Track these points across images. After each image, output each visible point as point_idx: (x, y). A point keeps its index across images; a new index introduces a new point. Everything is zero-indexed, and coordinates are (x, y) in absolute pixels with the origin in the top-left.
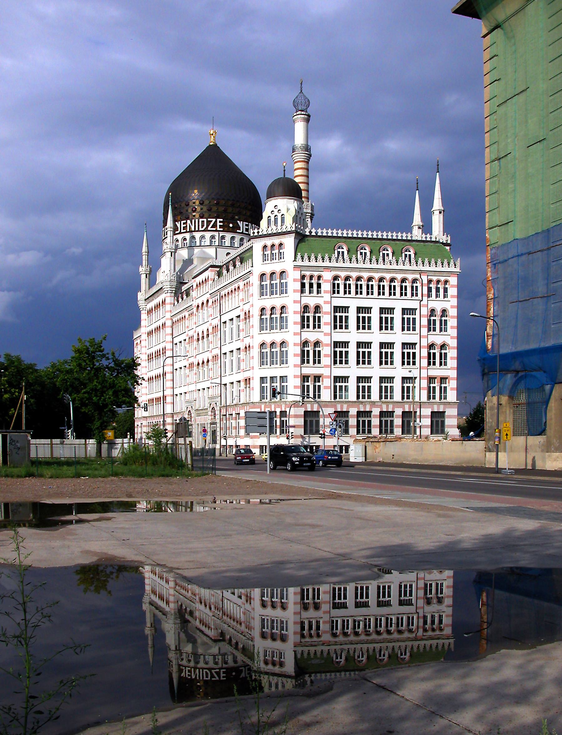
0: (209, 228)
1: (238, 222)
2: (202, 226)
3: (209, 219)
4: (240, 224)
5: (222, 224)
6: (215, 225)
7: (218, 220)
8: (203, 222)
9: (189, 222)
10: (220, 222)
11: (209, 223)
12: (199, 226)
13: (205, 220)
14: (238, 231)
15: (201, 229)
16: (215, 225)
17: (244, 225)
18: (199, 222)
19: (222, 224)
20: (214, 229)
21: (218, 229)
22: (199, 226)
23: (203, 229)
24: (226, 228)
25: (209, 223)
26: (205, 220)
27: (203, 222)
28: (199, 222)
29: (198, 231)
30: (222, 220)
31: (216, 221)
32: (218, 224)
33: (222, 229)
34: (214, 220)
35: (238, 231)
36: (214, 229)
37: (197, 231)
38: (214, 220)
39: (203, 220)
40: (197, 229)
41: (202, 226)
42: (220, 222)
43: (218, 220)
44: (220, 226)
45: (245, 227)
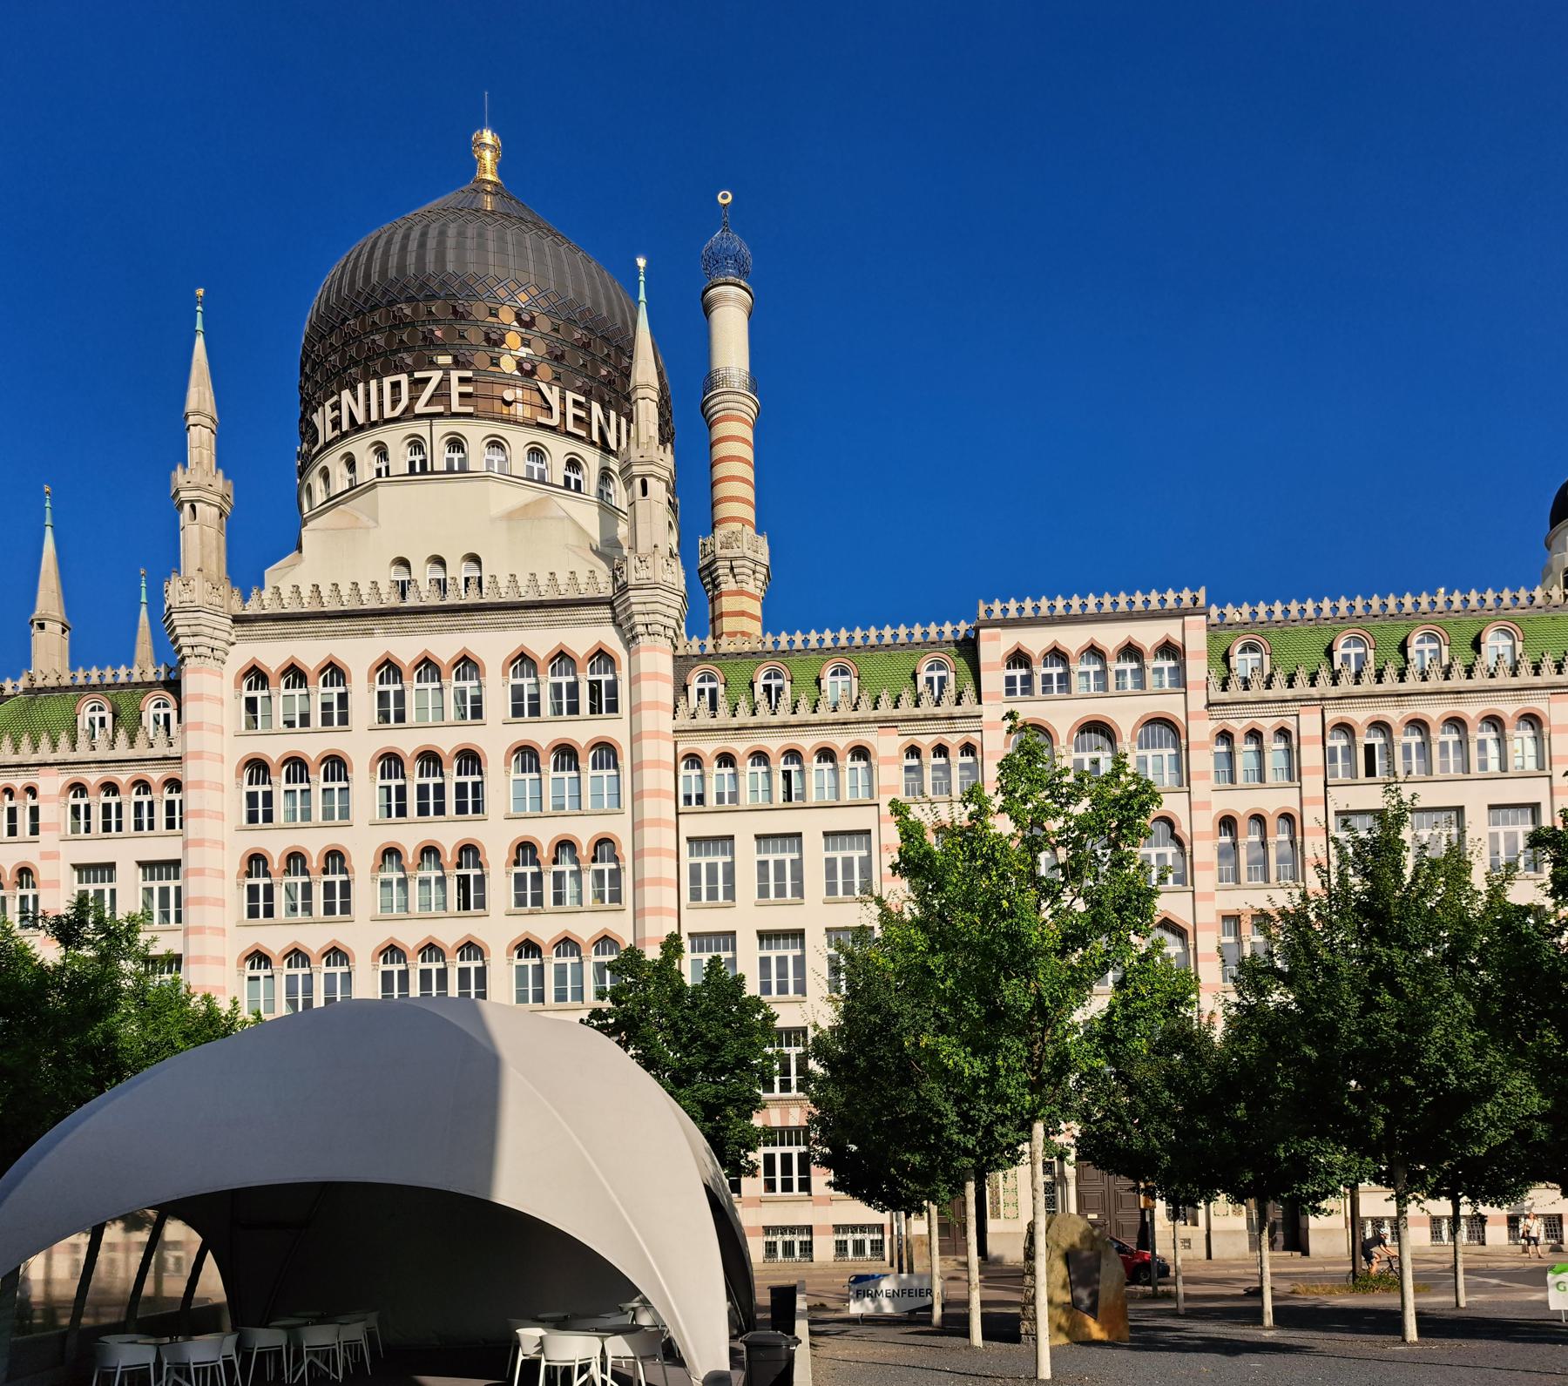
0: (420, 408)
1: (543, 387)
3: (417, 375)
4: (553, 396)
7: (455, 375)
8: (396, 386)
9: (346, 395)
12: (381, 405)
13: (404, 379)
14: (541, 420)
15: (388, 414)
16: (441, 394)
17: (569, 403)
18: (380, 390)
20: (440, 409)
21: (456, 408)
22: (381, 405)
23: (397, 413)
26: (404, 379)
27: (396, 386)
28: (380, 390)
32: (456, 389)
37: (374, 425)
39: (394, 378)
40: (374, 417)
43: (455, 375)
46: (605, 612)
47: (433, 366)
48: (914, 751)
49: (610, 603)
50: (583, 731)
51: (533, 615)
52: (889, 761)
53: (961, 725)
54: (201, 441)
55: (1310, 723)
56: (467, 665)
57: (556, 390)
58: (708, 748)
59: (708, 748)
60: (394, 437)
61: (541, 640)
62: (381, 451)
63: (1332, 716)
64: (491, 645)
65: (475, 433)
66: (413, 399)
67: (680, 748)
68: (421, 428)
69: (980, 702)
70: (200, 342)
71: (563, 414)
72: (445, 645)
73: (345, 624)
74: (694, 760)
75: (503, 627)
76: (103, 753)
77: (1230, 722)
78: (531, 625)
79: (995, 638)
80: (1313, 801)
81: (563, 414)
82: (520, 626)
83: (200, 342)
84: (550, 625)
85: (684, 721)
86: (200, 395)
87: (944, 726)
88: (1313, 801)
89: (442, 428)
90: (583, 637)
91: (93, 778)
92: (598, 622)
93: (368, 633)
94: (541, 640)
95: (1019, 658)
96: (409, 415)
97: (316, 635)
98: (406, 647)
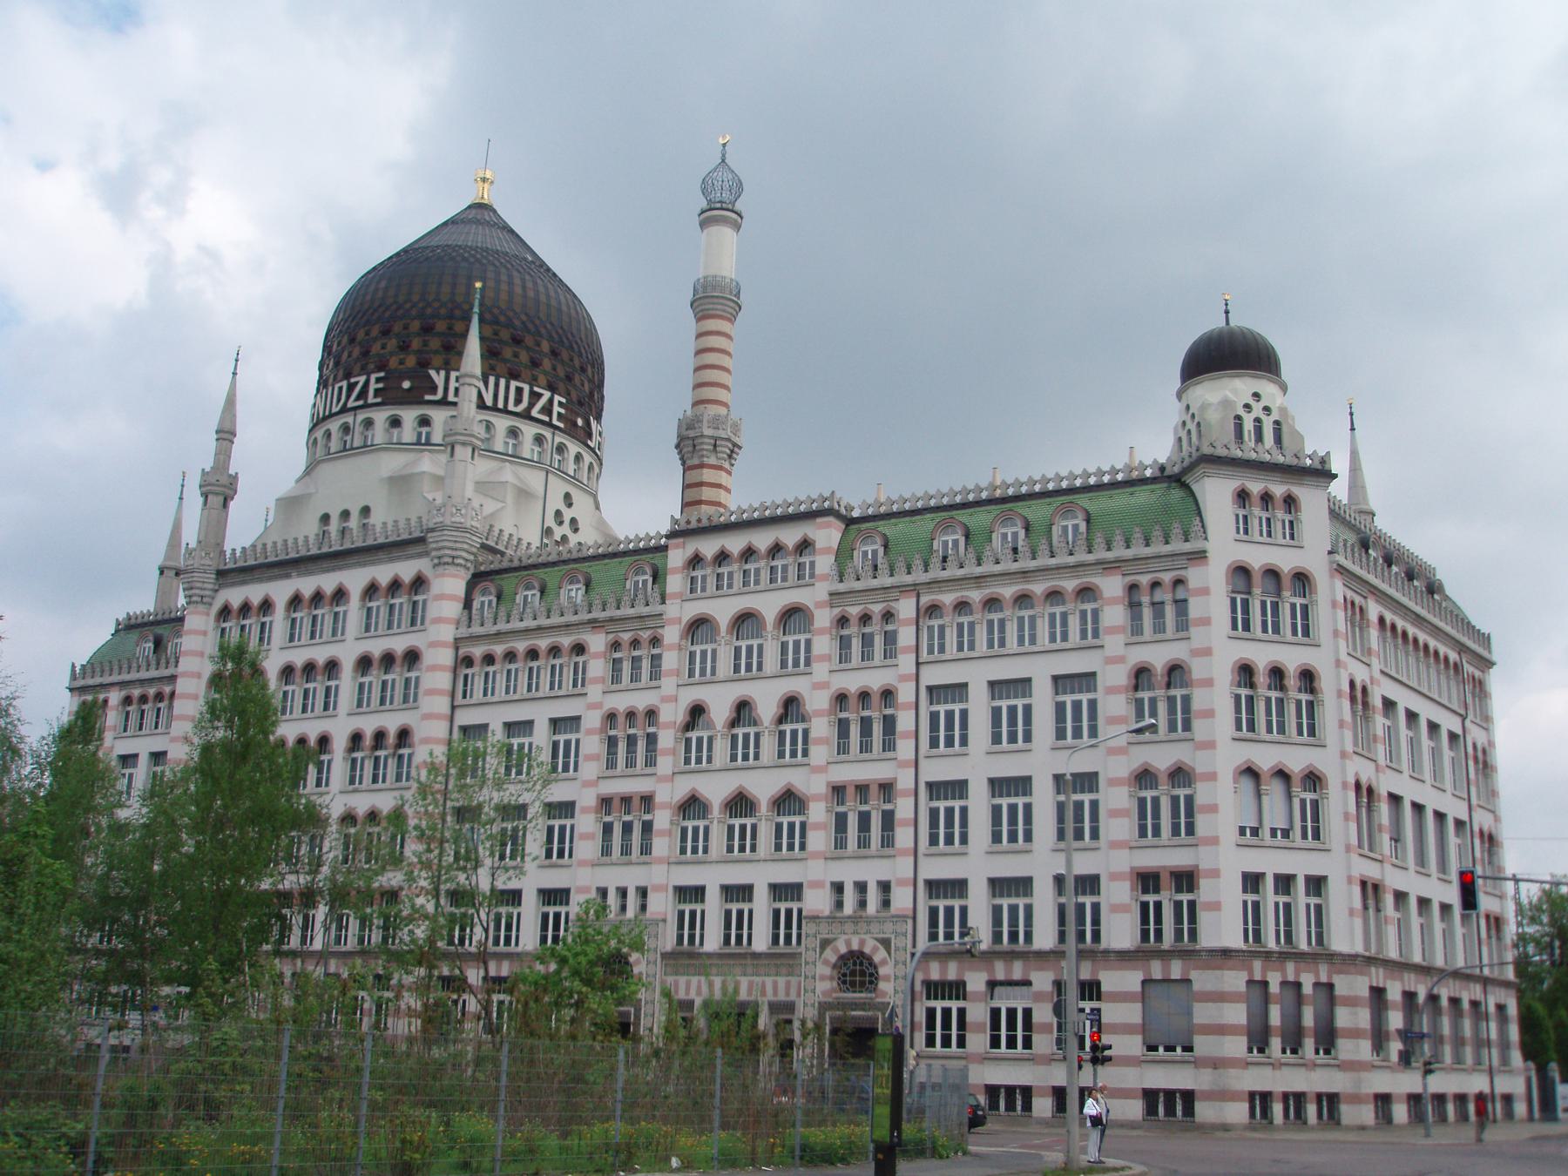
1: (432, 373)
2: (339, 400)
6: (363, 394)
10: (378, 380)
11: (351, 387)
13: (344, 384)
14: (428, 397)
19: (380, 385)
20: (361, 403)
21: (371, 400)
24: (390, 396)
25: (351, 387)
26: (344, 384)
29: (332, 415)
30: (382, 374)
31: (367, 384)
32: (373, 386)
33: (379, 400)
34: (362, 379)
35: (428, 397)
36: (361, 403)
38: (362, 379)
41: (339, 400)
42: (378, 380)
44: (377, 392)
45: (453, 385)
46: (419, 549)
47: (365, 370)
48: (616, 646)
49: (421, 540)
50: (399, 645)
51: (381, 555)
52: (596, 656)
53: (651, 623)
55: (906, 608)
56: (340, 595)
57: (443, 373)
58: (478, 651)
59: (478, 651)
60: (334, 426)
61: (383, 573)
62: (328, 435)
63: (926, 599)
64: (355, 579)
65: (381, 417)
66: (348, 397)
67: (461, 652)
68: (349, 418)
69: (663, 602)
71: (446, 389)
72: (328, 582)
73: (276, 571)
74: (468, 661)
75: (364, 565)
76: (144, 675)
77: (871, 607)
78: (380, 562)
79: (677, 547)
80: (903, 678)
81: (446, 389)
82: (373, 563)
84: (391, 560)
85: (464, 632)
87: (636, 625)
88: (903, 678)
89: (361, 416)
90: (405, 570)
91: (136, 692)
92: (420, 555)
93: (288, 576)
94: (383, 573)
95: (696, 561)
96: (344, 410)
97: (260, 580)
98: (306, 585)
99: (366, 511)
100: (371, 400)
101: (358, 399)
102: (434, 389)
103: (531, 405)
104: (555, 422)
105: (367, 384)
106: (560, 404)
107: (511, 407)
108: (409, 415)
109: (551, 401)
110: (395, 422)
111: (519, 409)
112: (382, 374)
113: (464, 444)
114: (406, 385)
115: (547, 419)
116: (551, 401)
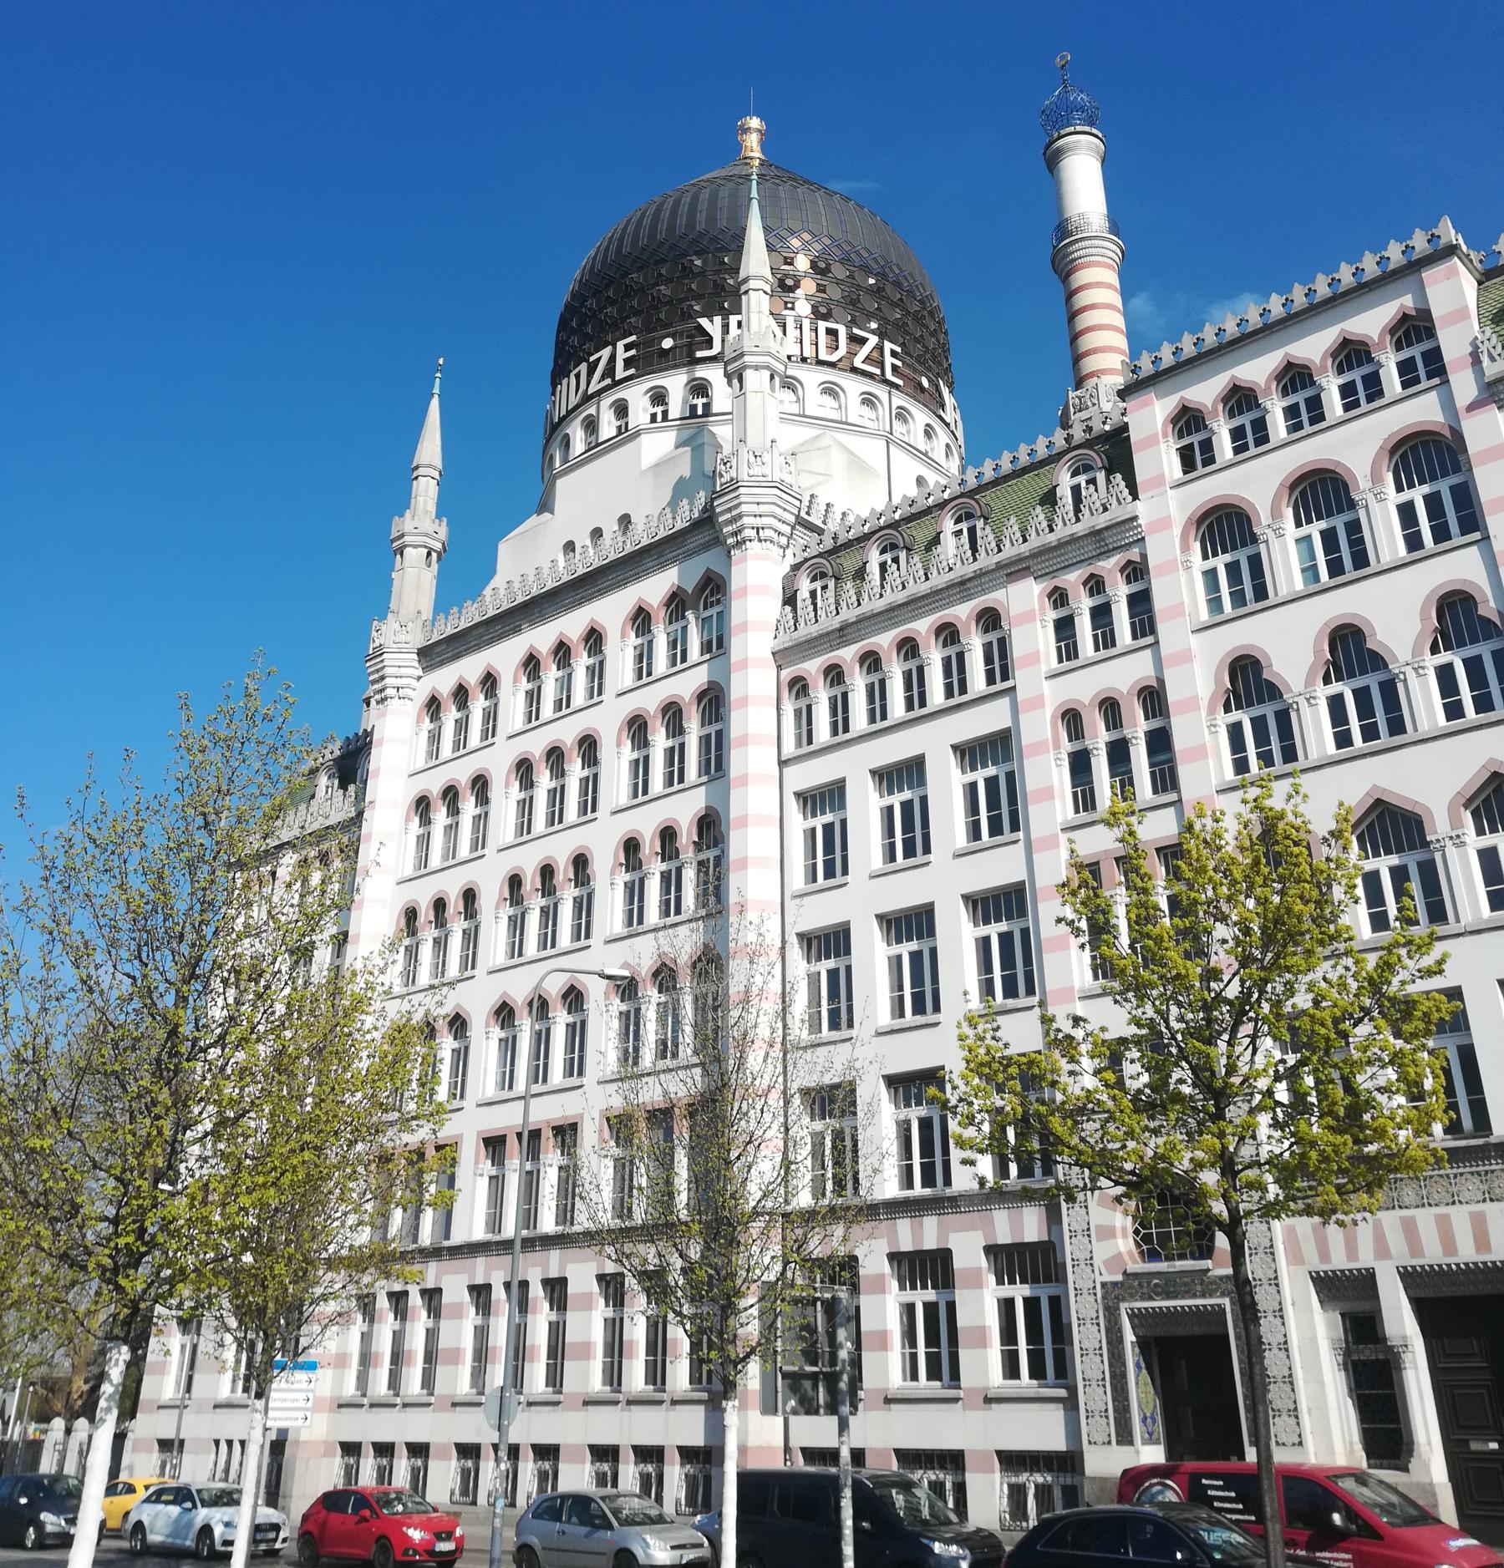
1: (704, 322)
3: (592, 359)
5: (633, 352)
10: (627, 348)
13: (583, 367)
14: (699, 354)
19: (633, 352)
20: (608, 381)
24: (647, 361)
26: (583, 367)
27: (578, 376)
30: (633, 338)
31: (613, 358)
32: (621, 355)
33: (632, 371)
36: (608, 381)
38: (605, 353)
44: (628, 363)
54: (426, 492)
65: (637, 395)
66: (588, 384)
70: (435, 403)
83: (435, 403)
86: (430, 449)
92: (706, 547)
93: (517, 630)
99: (625, 521)
100: (620, 373)
101: (603, 378)
102: (709, 343)
103: (852, 354)
104: (889, 375)
105: (613, 358)
106: (894, 354)
107: (823, 356)
108: (675, 383)
109: (880, 348)
110: (659, 397)
111: (834, 358)
112: (633, 338)
113: (757, 368)
114: (667, 343)
115: (878, 371)
116: (880, 348)
